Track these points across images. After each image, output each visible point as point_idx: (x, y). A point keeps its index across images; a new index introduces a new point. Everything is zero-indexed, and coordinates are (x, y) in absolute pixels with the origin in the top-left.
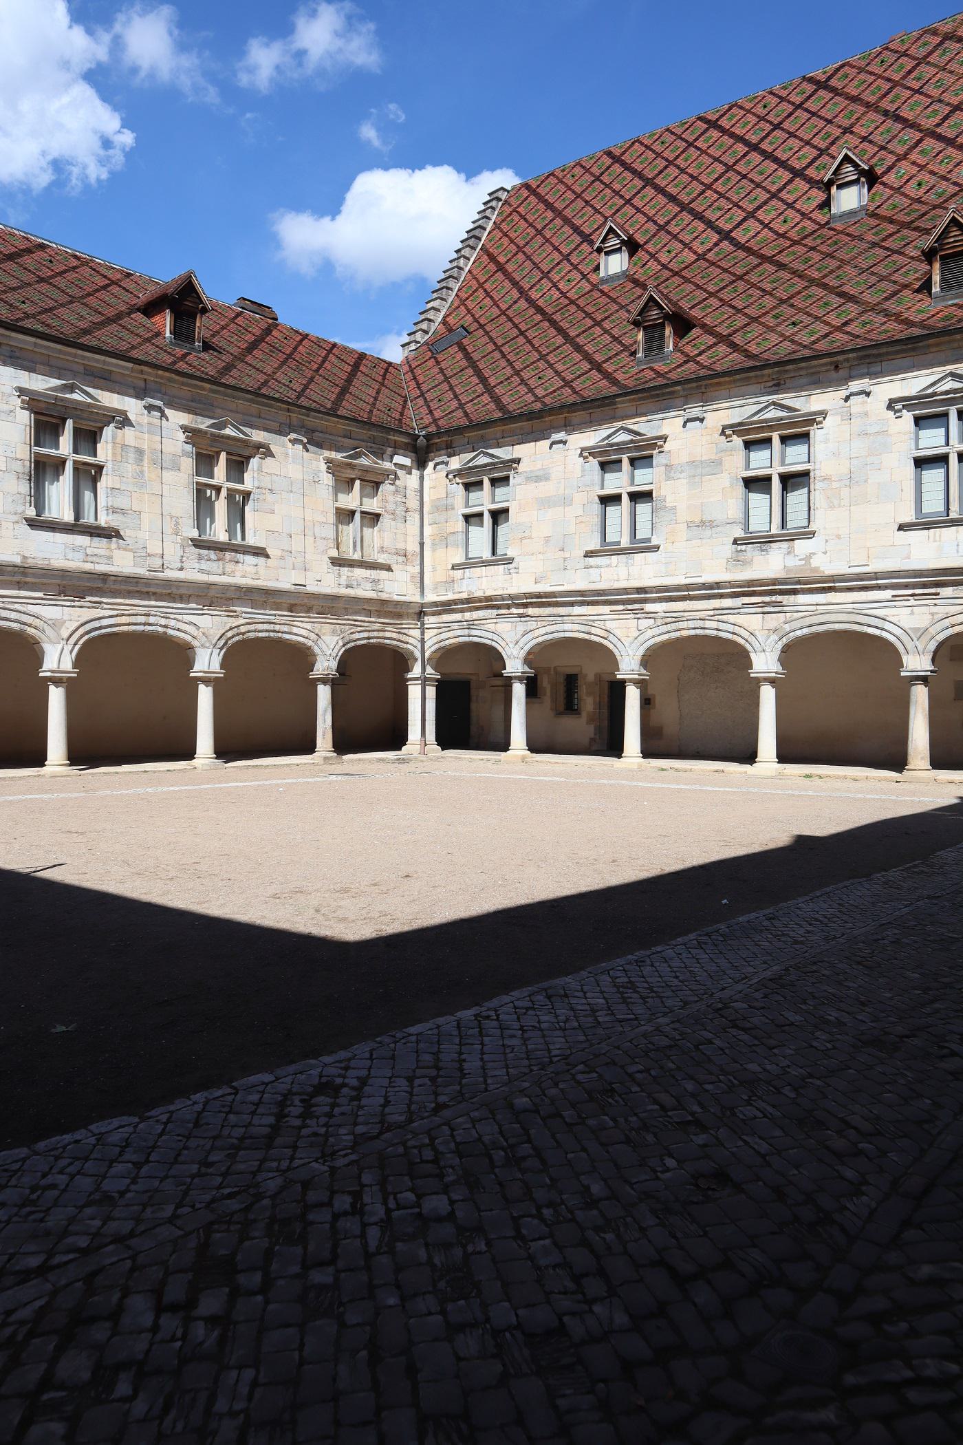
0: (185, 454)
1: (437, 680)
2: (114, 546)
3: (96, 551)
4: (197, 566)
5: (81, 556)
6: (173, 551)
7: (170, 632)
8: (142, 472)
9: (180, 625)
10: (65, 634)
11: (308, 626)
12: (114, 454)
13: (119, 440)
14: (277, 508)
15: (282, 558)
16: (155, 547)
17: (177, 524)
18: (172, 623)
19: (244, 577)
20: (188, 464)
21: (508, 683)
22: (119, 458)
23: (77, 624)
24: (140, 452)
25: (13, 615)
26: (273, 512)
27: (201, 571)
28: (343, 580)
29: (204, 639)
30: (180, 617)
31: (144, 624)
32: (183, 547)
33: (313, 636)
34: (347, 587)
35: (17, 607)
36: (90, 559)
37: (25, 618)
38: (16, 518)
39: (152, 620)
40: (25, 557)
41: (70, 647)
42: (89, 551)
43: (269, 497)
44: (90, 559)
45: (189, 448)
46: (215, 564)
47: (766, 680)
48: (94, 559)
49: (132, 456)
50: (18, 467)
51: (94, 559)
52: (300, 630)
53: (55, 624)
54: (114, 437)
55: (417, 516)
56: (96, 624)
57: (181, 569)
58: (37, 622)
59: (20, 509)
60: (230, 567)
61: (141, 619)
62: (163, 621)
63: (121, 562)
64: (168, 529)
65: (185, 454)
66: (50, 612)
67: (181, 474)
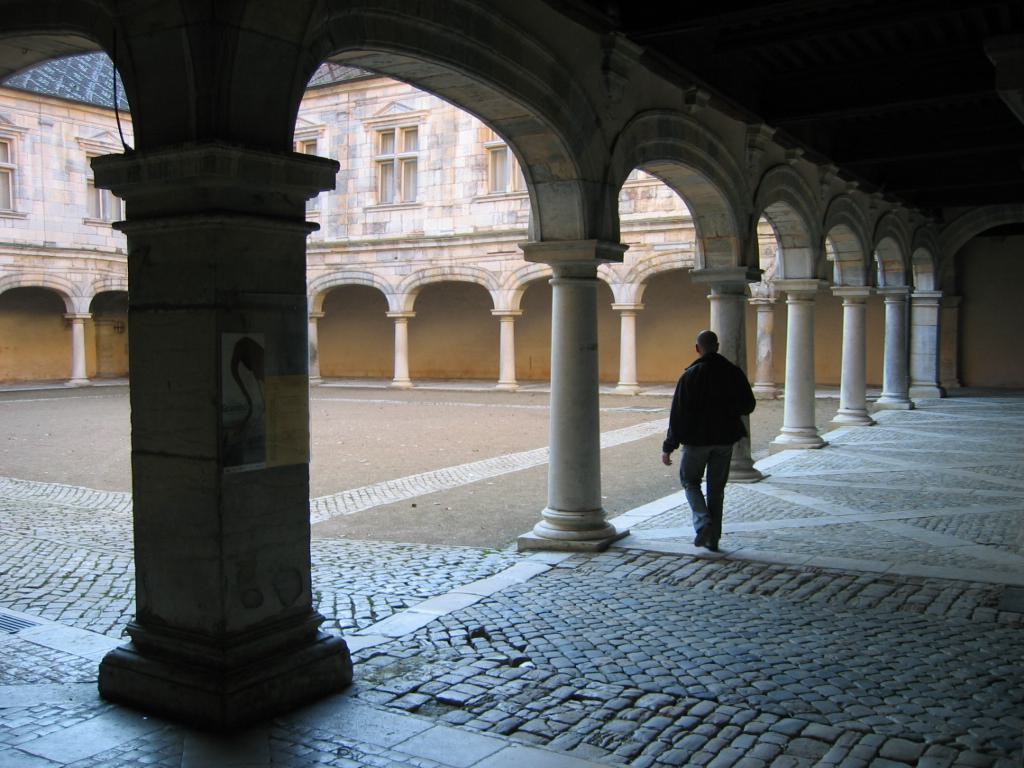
19: (654, 211)
23: (509, 273)
29: (615, 275)
35: (472, 265)
36: (520, 220)
37: (476, 273)
38: (470, 200)
40: (476, 228)
42: (519, 215)
44: (520, 220)
50: (472, 161)
58: (484, 275)
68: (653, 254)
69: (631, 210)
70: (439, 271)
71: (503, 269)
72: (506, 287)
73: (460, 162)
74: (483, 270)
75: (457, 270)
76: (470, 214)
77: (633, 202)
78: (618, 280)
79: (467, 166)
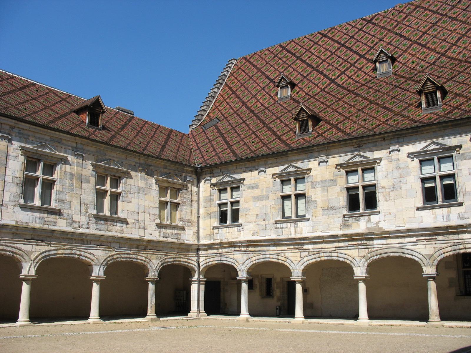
0: (92, 175)
1: (205, 281)
3: (50, 219)
4: (95, 227)
6: (84, 220)
8: (73, 184)
9: (86, 254)
10: (33, 258)
11: (145, 255)
12: (60, 175)
13: (63, 169)
14: (132, 200)
15: (134, 223)
16: (76, 218)
17: (87, 207)
18: (82, 253)
19: (116, 232)
20: (93, 180)
21: (239, 283)
22: (63, 177)
23: (38, 253)
24: (72, 175)
25: (9, 249)
26: (130, 202)
27: (97, 229)
28: (162, 234)
29: (97, 261)
30: (86, 251)
31: (70, 254)
32: (89, 218)
33: (147, 260)
34: (164, 237)
35: (11, 245)
36: (47, 223)
37: (15, 250)
38: (14, 204)
39: (73, 252)
40: (17, 222)
41: (34, 264)
42: (46, 219)
44: (47, 223)
45: (94, 173)
47: (361, 280)
48: (49, 223)
49: (68, 176)
50: (17, 181)
51: (49, 223)
52: (141, 257)
53: (28, 253)
54: (61, 168)
55: (196, 204)
56: (47, 253)
57: (88, 228)
58: (20, 252)
59: (17, 200)
60: (110, 227)
61: (68, 251)
63: (62, 225)
64: (83, 210)
65: (92, 175)
67: (90, 185)
69: (105, 230)
71: (34, 250)
72: (36, 261)
73: (9, 179)
76: (14, 212)
77: (106, 225)
78: (98, 264)
79: (13, 182)
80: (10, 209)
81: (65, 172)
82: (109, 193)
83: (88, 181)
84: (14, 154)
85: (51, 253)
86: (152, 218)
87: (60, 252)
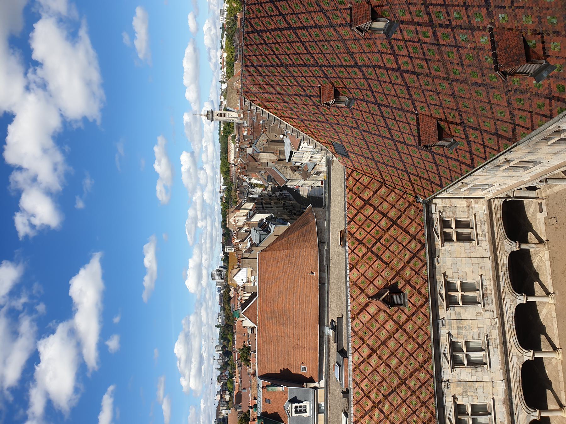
0: (454, 310)
2: (491, 337)
5: (496, 349)
7: (514, 315)
13: (456, 336)
15: (481, 268)
17: (478, 313)
20: (457, 309)
24: (458, 328)
27: (492, 303)
28: (483, 239)
37: (518, 369)
40: (500, 369)
43: (461, 274)
45: (452, 308)
46: (489, 298)
49: (460, 331)
50: (474, 371)
52: (504, 260)
53: (518, 358)
54: (456, 338)
55: (452, 200)
60: (489, 292)
62: (511, 318)
63: (495, 334)
64: (480, 317)
65: (454, 310)
66: (515, 359)
68: (506, 286)
70: (519, 389)
74: (517, 364)
75: (518, 379)
80: (493, 375)
81: (458, 334)
82: (463, 293)
83: (459, 313)
84: (456, 376)
85: (515, 340)
86: (473, 249)
87: (513, 333)
